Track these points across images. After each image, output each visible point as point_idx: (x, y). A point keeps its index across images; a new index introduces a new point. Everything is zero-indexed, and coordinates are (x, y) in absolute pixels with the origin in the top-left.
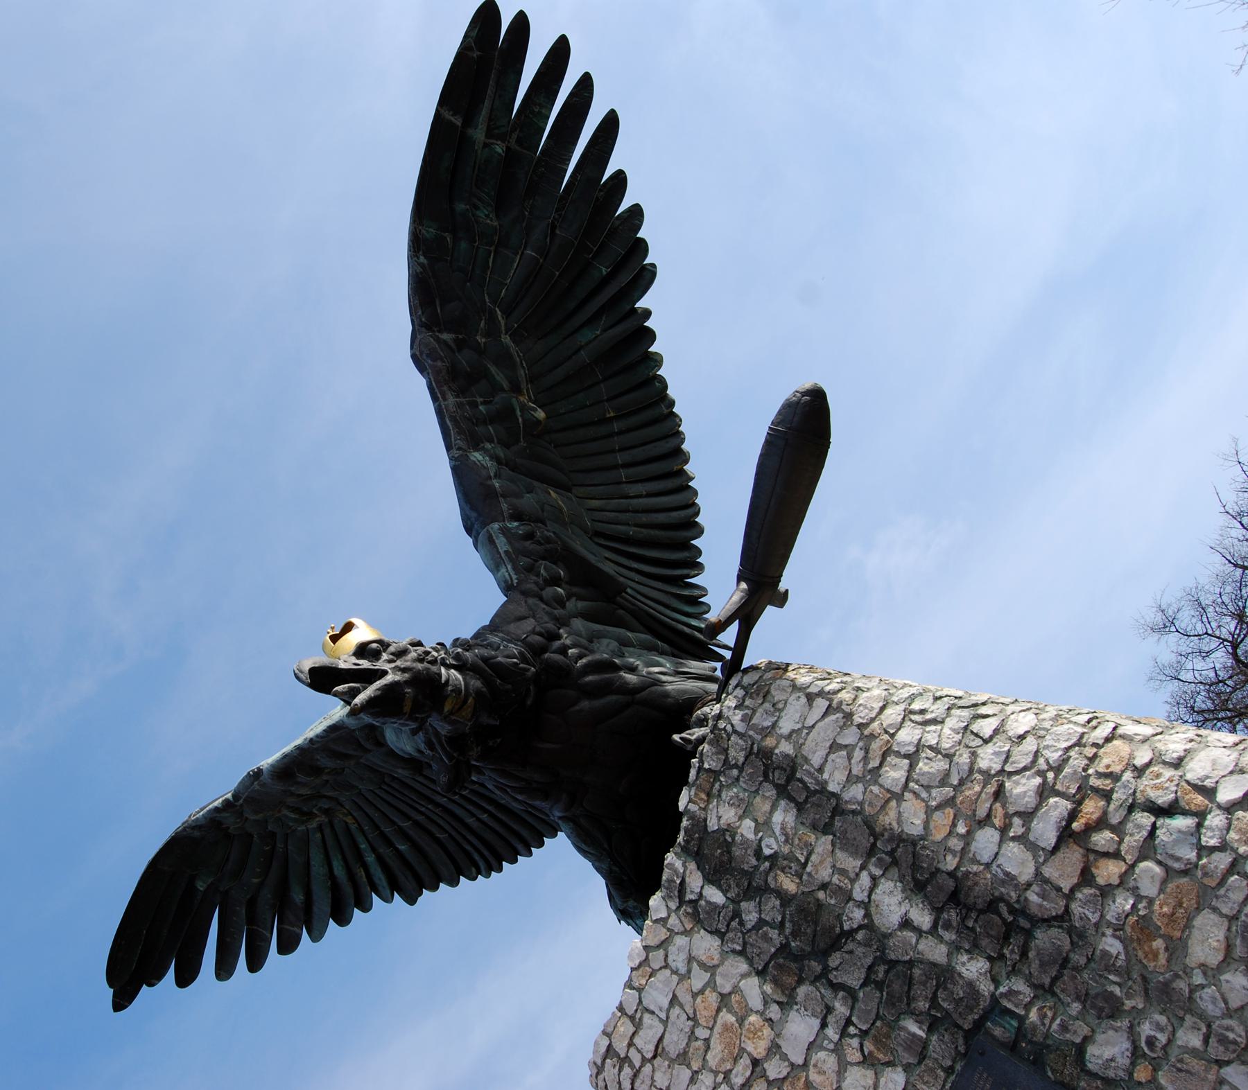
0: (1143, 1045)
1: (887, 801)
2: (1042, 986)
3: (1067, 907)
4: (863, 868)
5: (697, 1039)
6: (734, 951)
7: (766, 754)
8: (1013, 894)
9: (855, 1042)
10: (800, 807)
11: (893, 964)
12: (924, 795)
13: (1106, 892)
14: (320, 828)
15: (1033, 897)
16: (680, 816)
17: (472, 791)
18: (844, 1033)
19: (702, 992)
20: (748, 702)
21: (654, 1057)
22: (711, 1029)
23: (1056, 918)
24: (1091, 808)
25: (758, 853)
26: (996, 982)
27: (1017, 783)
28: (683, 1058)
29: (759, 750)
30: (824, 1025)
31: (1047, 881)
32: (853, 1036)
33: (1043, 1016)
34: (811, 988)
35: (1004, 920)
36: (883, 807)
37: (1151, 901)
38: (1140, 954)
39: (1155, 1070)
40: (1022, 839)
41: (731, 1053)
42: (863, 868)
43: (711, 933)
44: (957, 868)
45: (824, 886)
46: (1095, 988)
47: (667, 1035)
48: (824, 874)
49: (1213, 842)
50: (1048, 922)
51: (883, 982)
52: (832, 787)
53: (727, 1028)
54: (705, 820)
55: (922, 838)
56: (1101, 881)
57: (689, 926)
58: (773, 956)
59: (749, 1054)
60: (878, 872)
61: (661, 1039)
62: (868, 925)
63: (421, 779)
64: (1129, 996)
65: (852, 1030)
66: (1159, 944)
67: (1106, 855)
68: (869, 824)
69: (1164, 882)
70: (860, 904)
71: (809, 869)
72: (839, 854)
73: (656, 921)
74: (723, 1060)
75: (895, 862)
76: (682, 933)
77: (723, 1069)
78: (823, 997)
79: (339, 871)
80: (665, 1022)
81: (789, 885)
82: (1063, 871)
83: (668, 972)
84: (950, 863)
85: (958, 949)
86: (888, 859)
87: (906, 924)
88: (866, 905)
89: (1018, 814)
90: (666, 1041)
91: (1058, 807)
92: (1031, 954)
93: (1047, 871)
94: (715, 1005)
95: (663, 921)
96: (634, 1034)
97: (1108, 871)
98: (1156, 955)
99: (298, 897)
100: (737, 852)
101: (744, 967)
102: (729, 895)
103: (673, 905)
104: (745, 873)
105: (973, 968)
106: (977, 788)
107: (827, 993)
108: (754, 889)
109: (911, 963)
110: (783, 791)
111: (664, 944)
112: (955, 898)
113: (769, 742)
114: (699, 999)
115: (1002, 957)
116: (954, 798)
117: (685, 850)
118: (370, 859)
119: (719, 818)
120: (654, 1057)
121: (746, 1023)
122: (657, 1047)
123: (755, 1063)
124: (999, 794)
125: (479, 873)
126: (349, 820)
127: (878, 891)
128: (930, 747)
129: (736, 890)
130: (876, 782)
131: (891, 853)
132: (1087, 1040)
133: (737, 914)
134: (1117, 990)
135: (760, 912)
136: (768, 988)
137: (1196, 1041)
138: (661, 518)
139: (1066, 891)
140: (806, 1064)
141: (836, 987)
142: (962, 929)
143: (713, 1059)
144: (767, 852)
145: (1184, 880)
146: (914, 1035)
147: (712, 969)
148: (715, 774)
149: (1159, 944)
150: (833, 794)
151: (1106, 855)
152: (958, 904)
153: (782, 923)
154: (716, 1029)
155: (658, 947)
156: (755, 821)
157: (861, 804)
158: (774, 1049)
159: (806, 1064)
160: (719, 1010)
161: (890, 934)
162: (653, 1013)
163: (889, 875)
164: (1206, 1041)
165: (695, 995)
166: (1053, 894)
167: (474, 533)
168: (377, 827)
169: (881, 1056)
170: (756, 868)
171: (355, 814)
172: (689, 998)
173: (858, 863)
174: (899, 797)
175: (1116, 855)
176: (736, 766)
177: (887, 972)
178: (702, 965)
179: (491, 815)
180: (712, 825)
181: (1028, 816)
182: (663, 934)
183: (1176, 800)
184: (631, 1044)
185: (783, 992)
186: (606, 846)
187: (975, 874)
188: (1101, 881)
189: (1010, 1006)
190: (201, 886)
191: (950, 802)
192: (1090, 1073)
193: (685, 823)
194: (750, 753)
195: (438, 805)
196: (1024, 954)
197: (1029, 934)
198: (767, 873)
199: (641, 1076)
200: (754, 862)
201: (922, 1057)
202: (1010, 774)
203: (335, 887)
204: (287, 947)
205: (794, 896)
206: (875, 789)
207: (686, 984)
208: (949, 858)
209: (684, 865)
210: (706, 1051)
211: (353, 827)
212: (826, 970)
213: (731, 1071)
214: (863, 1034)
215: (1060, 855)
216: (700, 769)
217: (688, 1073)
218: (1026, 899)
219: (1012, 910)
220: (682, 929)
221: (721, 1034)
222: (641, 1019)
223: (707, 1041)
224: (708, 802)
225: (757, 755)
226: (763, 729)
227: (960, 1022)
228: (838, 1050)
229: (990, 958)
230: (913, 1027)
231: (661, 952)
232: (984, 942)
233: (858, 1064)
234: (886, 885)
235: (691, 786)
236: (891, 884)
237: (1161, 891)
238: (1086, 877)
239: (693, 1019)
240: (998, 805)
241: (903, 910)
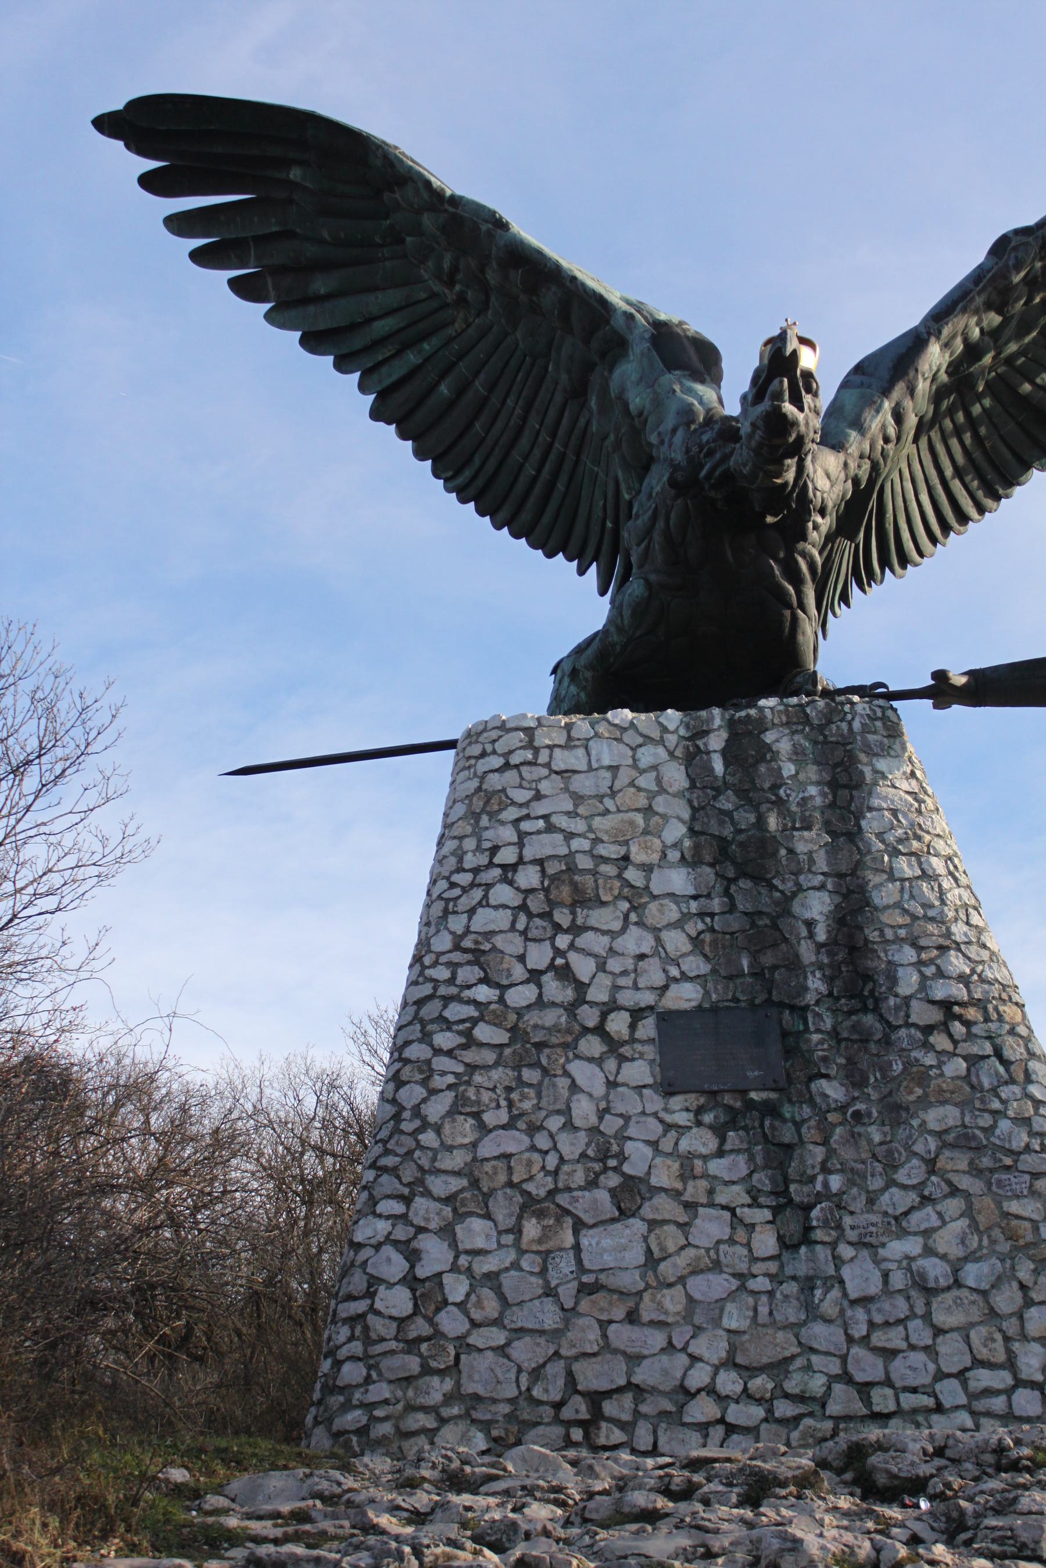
0: (850, 1111)
1: (883, 871)
2: (838, 1034)
3: (900, 1027)
4: (823, 874)
5: (601, 802)
6: (690, 802)
7: (853, 759)
8: (884, 989)
9: (701, 926)
10: (833, 805)
11: (775, 927)
12: (906, 896)
13: (927, 1046)
14: (433, 295)
15: (892, 1001)
16: (754, 705)
17: (562, 457)
18: (701, 915)
19: (639, 789)
20: (879, 724)
21: (557, 773)
22: (619, 811)
23: (888, 1022)
24: (972, 1013)
25: (775, 787)
26: (818, 1003)
27: (957, 957)
28: (578, 798)
29: (850, 751)
30: (695, 898)
31: (908, 1006)
32: (703, 922)
33: (821, 1042)
34: (712, 876)
35: (862, 990)
36: (877, 870)
37: (942, 1075)
38: (905, 1083)
39: (841, 1124)
40: (923, 977)
41: (616, 836)
42: (823, 874)
43: (688, 775)
44: (874, 943)
45: (791, 851)
46: (864, 1065)
47: (582, 775)
48: (801, 848)
49: (1003, 1096)
50: (882, 1019)
51: (757, 926)
52: (863, 823)
53: (632, 823)
54: (767, 730)
55: (876, 909)
56: (932, 1039)
57: (678, 753)
58: (711, 835)
59: (628, 850)
60: (830, 887)
61: (575, 772)
62: (788, 899)
63: (559, 398)
64: (874, 1088)
65: (708, 920)
66: (919, 1092)
67: (950, 1036)
68: (858, 865)
69: (958, 1077)
70: (797, 884)
71: (795, 833)
72: (822, 852)
73: (660, 724)
74: (607, 832)
75: (845, 897)
76: (668, 750)
77: (600, 835)
78: (713, 887)
79: (382, 327)
80: (590, 769)
81: (773, 822)
82: (922, 1014)
83: (630, 753)
84: (874, 936)
85: (821, 968)
86: (844, 891)
87: (810, 924)
88: (800, 889)
89: (938, 967)
90: (576, 776)
91: (959, 992)
92: (854, 1018)
93: (914, 1003)
94: (639, 806)
95: (665, 729)
96: (559, 746)
97: (941, 1041)
98: (911, 1092)
99: (320, 285)
100: (763, 768)
101: (686, 815)
102: (728, 777)
103: (682, 732)
104: (752, 782)
105: (816, 984)
106: (936, 932)
107: (719, 888)
108: (748, 795)
109: (786, 940)
110: (834, 785)
111: (648, 739)
112: (853, 949)
113: (863, 757)
114: (633, 790)
115: (838, 999)
116: (918, 918)
117: (731, 724)
118: (412, 358)
119: (777, 741)
120: (557, 773)
121: (649, 837)
122: (567, 771)
123: (626, 858)
124: (943, 949)
125: (446, 480)
126: (458, 325)
127: (817, 894)
128: (940, 886)
129: (736, 781)
130: (890, 856)
131: (850, 892)
132: (826, 1076)
133: (718, 792)
134: (872, 1080)
135: (736, 809)
136: (687, 843)
137: (877, 1138)
138: (906, 535)
139: (910, 1021)
140: (655, 897)
141: (727, 893)
142: (835, 966)
143: (597, 822)
144: (782, 792)
145: (968, 1089)
146: (742, 966)
147: (662, 790)
148: (807, 720)
149: (919, 1092)
150: (860, 827)
151: (950, 1036)
152: (849, 954)
153: (741, 831)
154: (621, 815)
155: (642, 735)
156: (797, 773)
157: (869, 852)
158: (647, 869)
159: (655, 897)
160: (638, 810)
161: (794, 917)
162: (589, 755)
163: (834, 896)
164: (881, 1144)
165: (632, 784)
166: (902, 1014)
167: (858, 379)
168: (461, 357)
169: (707, 949)
170: (763, 790)
171: (471, 331)
172: (627, 781)
173: (826, 869)
174: (892, 878)
175: (955, 1043)
176: (825, 737)
177: (766, 926)
178: (659, 781)
179: (535, 479)
180: (769, 737)
181: (941, 974)
182: (656, 734)
183: (1012, 1063)
184: (548, 747)
185: (693, 856)
186: (638, 633)
187: (879, 957)
188: (932, 1039)
189: (810, 1020)
190: (295, 174)
191: (915, 918)
192: (808, 1088)
193: (753, 712)
194: (844, 745)
195: (524, 419)
196: (850, 1013)
197: (865, 1010)
198: (768, 801)
199: (534, 768)
200: (767, 785)
201: (730, 978)
202: (959, 950)
203: (353, 327)
204: (241, 288)
205: (767, 831)
206: (886, 858)
207: (634, 773)
208: (876, 933)
209: (720, 727)
210: (599, 815)
211: (450, 331)
212: (734, 880)
213: (603, 842)
214: (712, 930)
215: (930, 1006)
216: (800, 705)
217: (570, 807)
218: (887, 998)
219: (872, 992)
220: (672, 749)
221: (622, 821)
222: (575, 746)
223: (607, 812)
224: (782, 725)
225: (846, 751)
226: (869, 746)
227: (774, 993)
228: (686, 917)
229: (830, 994)
230: (745, 963)
231: (640, 740)
232: (838, 983)
233: (688, 935)
234: (825, 897)
235: (782, 703)
236: (828, 900)
237: (952, 1078)
238: (928, 1030)
239: (613, 794)
240: (935, 952)
241: (817, 918)
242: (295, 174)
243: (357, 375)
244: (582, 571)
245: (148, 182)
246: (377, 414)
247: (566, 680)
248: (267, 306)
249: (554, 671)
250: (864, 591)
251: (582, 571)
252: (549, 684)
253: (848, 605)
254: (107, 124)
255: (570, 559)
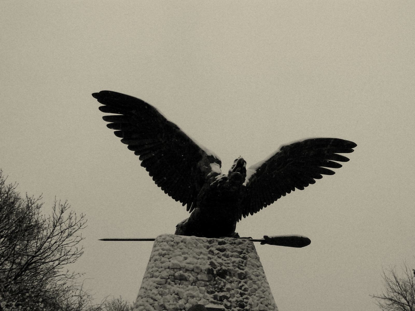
190: (134, 112)
204: (116, 133)
242: (134, 112)
243: (139, 156)
244: (183, 205)
245: (101, 109)
246: (142, 165)
247: (179, 229)
248: (122, 138)
249: (177, 226)
250: (245, 217)
251: (183, 205)
252: (175, 229)
253: (241, 220)
254: (95, 95)
255: (181, 202)
